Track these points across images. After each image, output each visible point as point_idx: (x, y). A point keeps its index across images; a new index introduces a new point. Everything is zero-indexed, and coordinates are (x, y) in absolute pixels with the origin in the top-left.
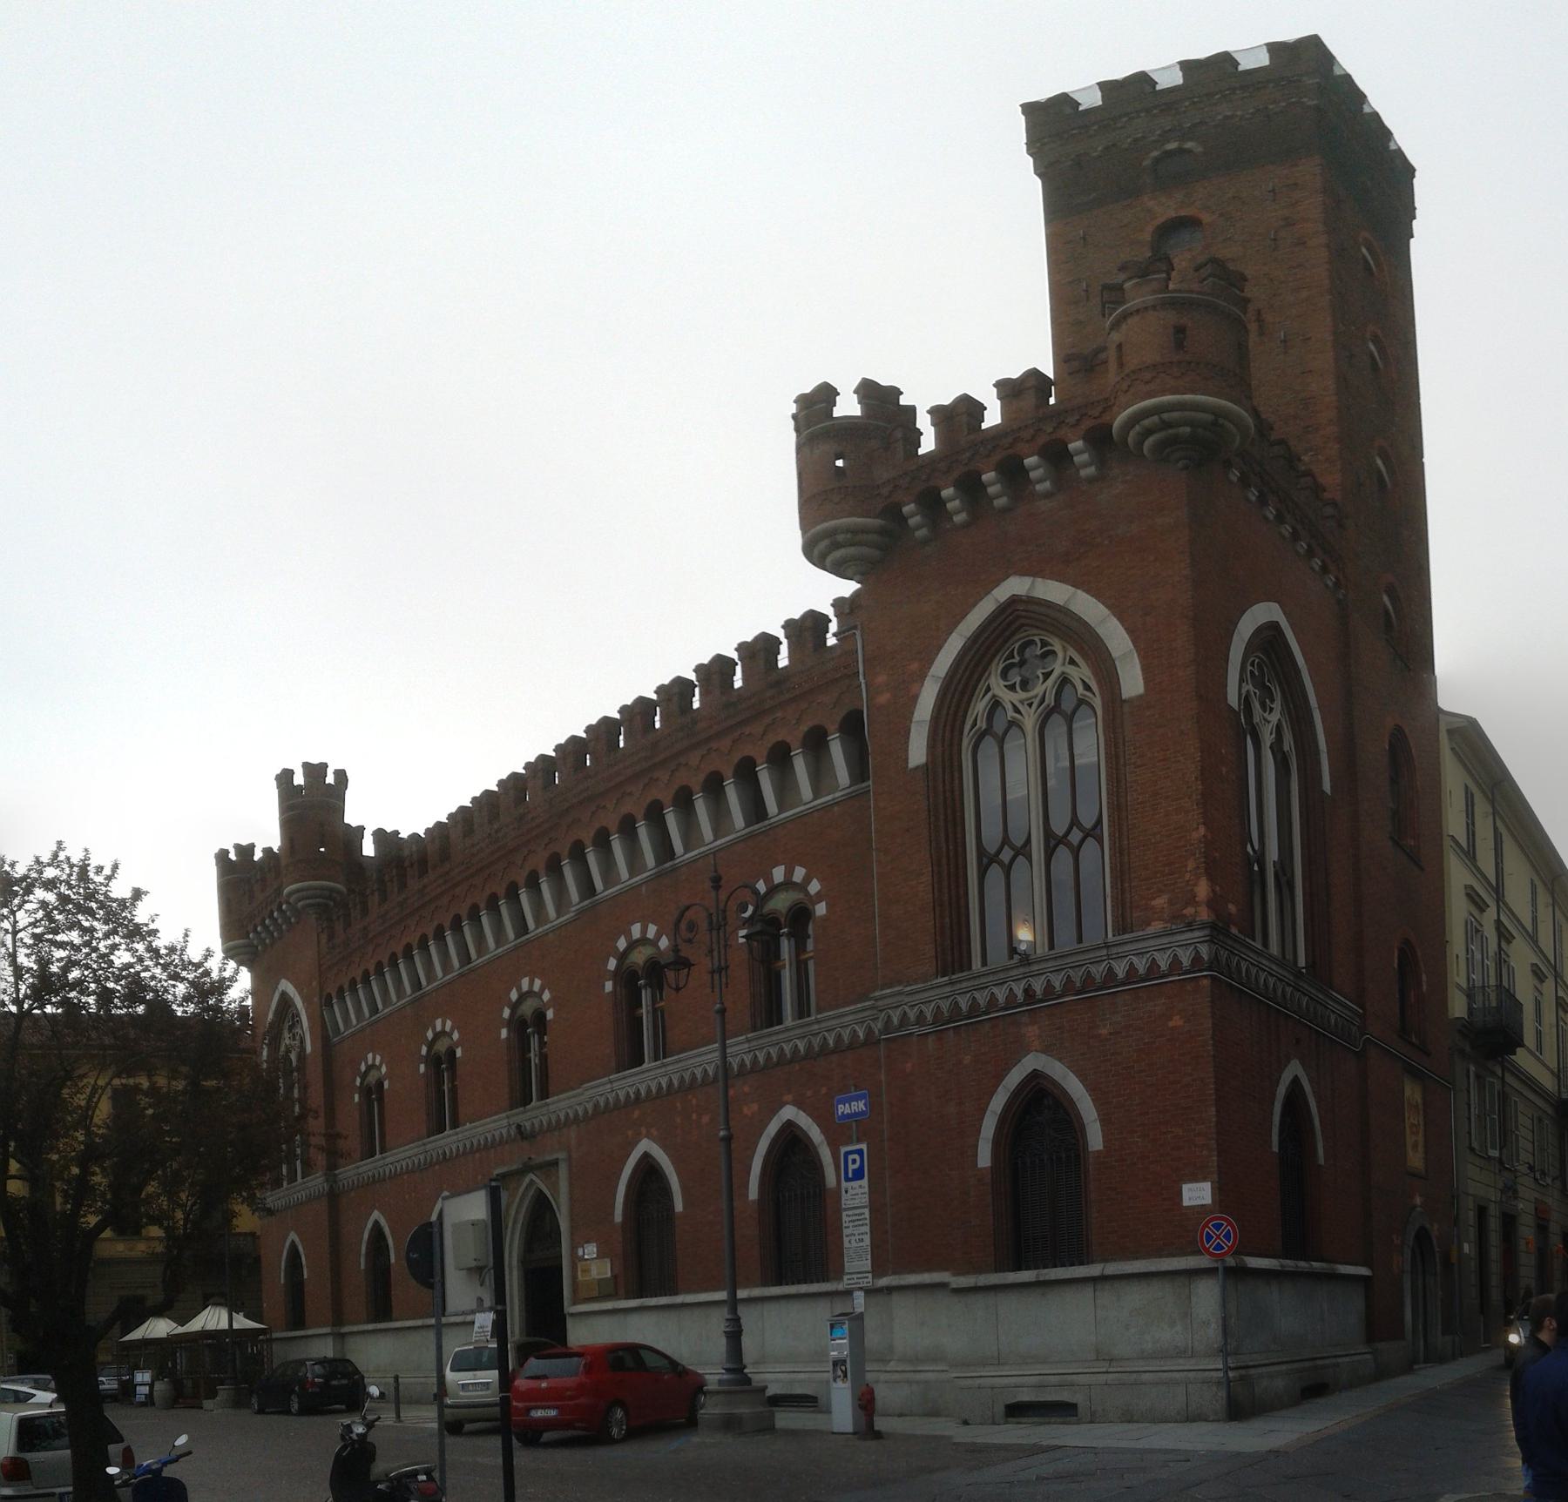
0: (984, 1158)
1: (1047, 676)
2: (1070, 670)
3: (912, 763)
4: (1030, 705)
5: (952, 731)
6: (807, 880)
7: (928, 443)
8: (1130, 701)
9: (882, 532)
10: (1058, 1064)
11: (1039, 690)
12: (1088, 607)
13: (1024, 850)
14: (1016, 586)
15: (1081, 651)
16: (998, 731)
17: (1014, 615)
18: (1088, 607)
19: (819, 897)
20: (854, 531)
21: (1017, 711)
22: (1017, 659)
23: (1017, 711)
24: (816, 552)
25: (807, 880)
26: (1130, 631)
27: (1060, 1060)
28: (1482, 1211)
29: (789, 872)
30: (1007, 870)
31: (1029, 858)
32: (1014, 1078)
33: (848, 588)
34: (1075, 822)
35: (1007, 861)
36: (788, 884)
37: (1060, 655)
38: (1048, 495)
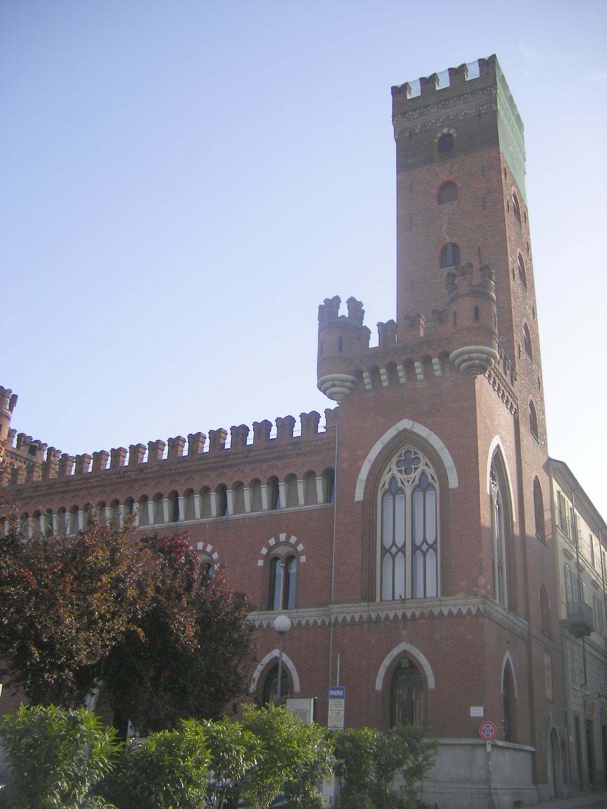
0: (379, 686)
1: (416, 469)
2: (426, 468)
3: (357, 499)
4: (408, 482)
5: (374, 487)
6: (297, 543)
7: (374, 342)
8: (453, 490)
9: (352, 382)
10: (415, 649)
11: (412, 475)
12: (436, 442)
13: (402, 550)
14: (405, 424)
15: (430, 460)
16: (394, 490)
17: (405, 436)
18: (436, 442)
19: (303, 553)
20: (343, 381)
21: (402, 483)
22: (403, 459)
23: (402, 483)
24: (324, 386)
25: (297, 543)
26: (453, 457)
27: (416, 647)
28: (577, 719)
29: (288, 537)
30: (394, 557)
31: (404, 553)
32: (395, 652)
33: (333, 405)
34: (425, 540)
35: (394, 553)
36: (287, 543)
37: (422, 460)
38: (421, 381)
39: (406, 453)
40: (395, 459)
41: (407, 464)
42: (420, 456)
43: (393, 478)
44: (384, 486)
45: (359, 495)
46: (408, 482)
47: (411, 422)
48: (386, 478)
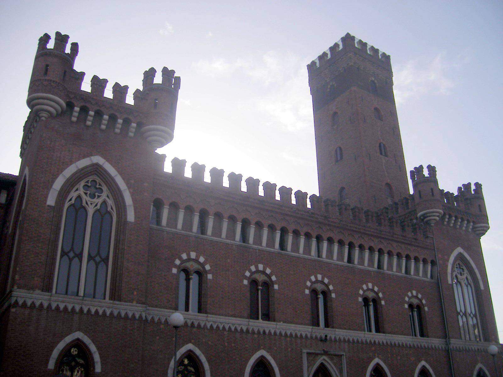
2: (107, 199)
4: (91, 204)
11: (96, 200)
14: (97, 159)
23: (87, 203)
32: (68, 339)
39: (92, 181)
40: (82, 183)
41: (94, 190)
42: (103, 188)
43: (79, 197)
44: (71, 200)
45: (51, 201)
46: (91, 204)
47: (88, 159)
48: (73, 195)
